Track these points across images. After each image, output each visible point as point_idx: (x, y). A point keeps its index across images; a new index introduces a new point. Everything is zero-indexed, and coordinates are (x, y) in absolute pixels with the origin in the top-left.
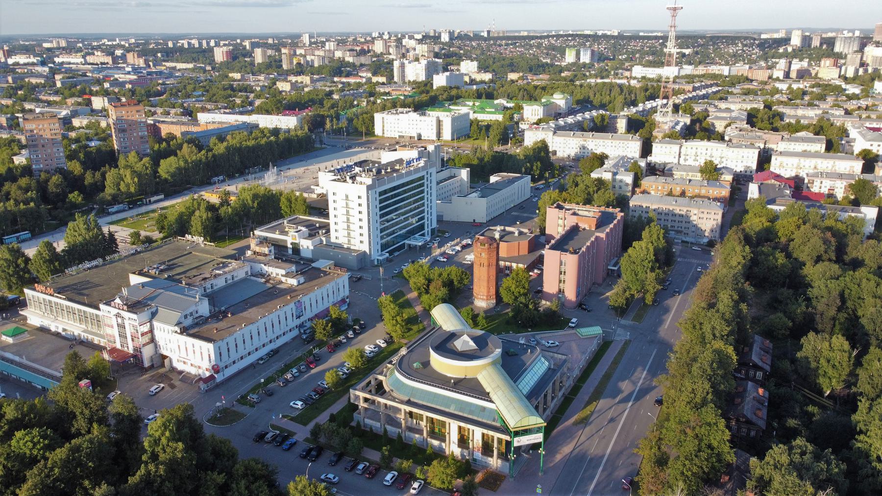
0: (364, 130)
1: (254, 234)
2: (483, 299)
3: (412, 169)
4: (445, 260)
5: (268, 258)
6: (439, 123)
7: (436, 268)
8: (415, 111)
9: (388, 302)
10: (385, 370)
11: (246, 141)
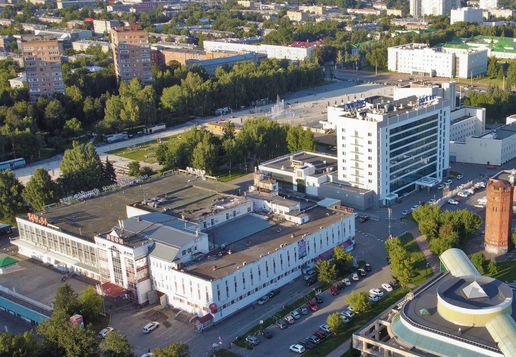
0: (377, 64)
1: (258, 169)
2: (494, 245)
3: (425, 107)
4: (456, 203)
5: (272, 194)
6: (455, 60)
7: (447, 211)
8: (430, 46)
9: (395, 244)
10: (390, 315)
11: (253, 72)
